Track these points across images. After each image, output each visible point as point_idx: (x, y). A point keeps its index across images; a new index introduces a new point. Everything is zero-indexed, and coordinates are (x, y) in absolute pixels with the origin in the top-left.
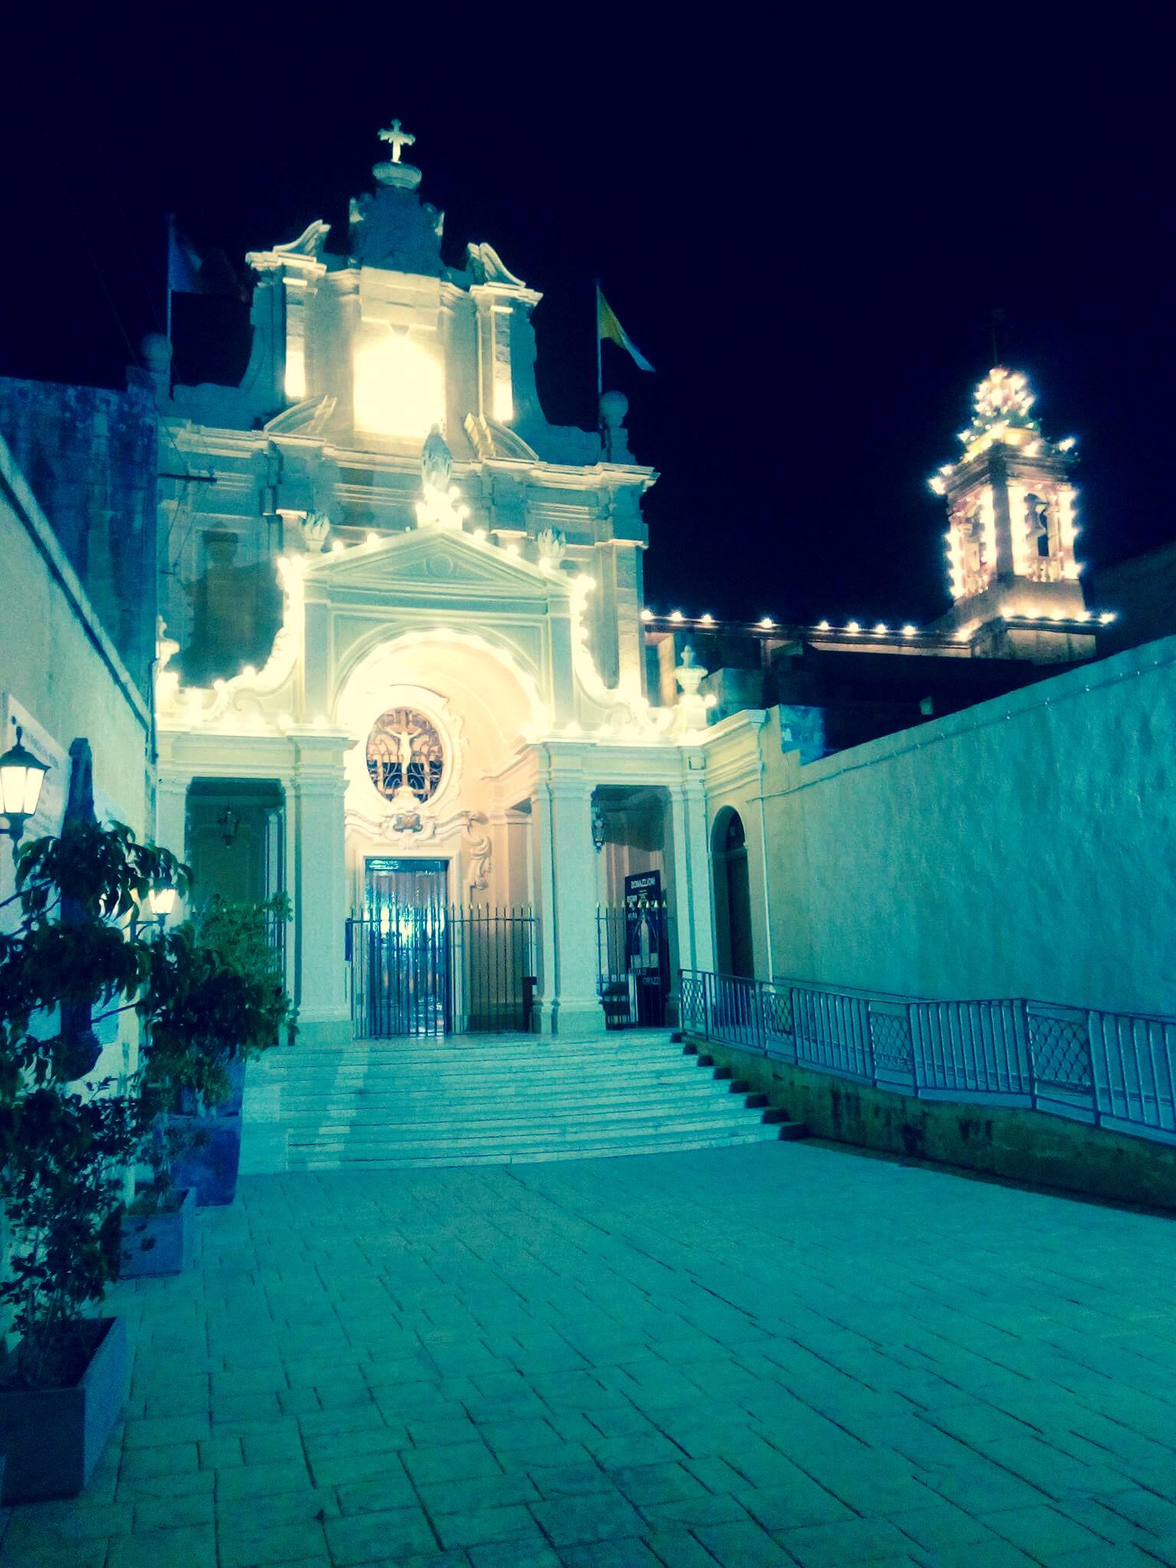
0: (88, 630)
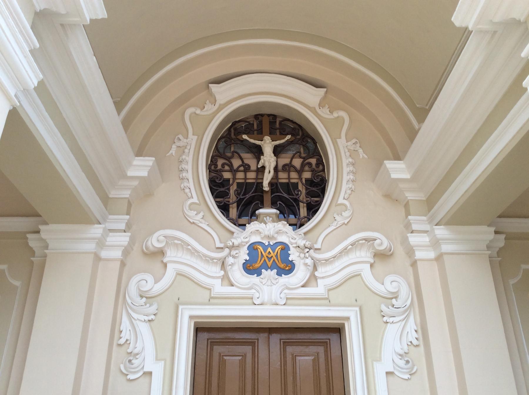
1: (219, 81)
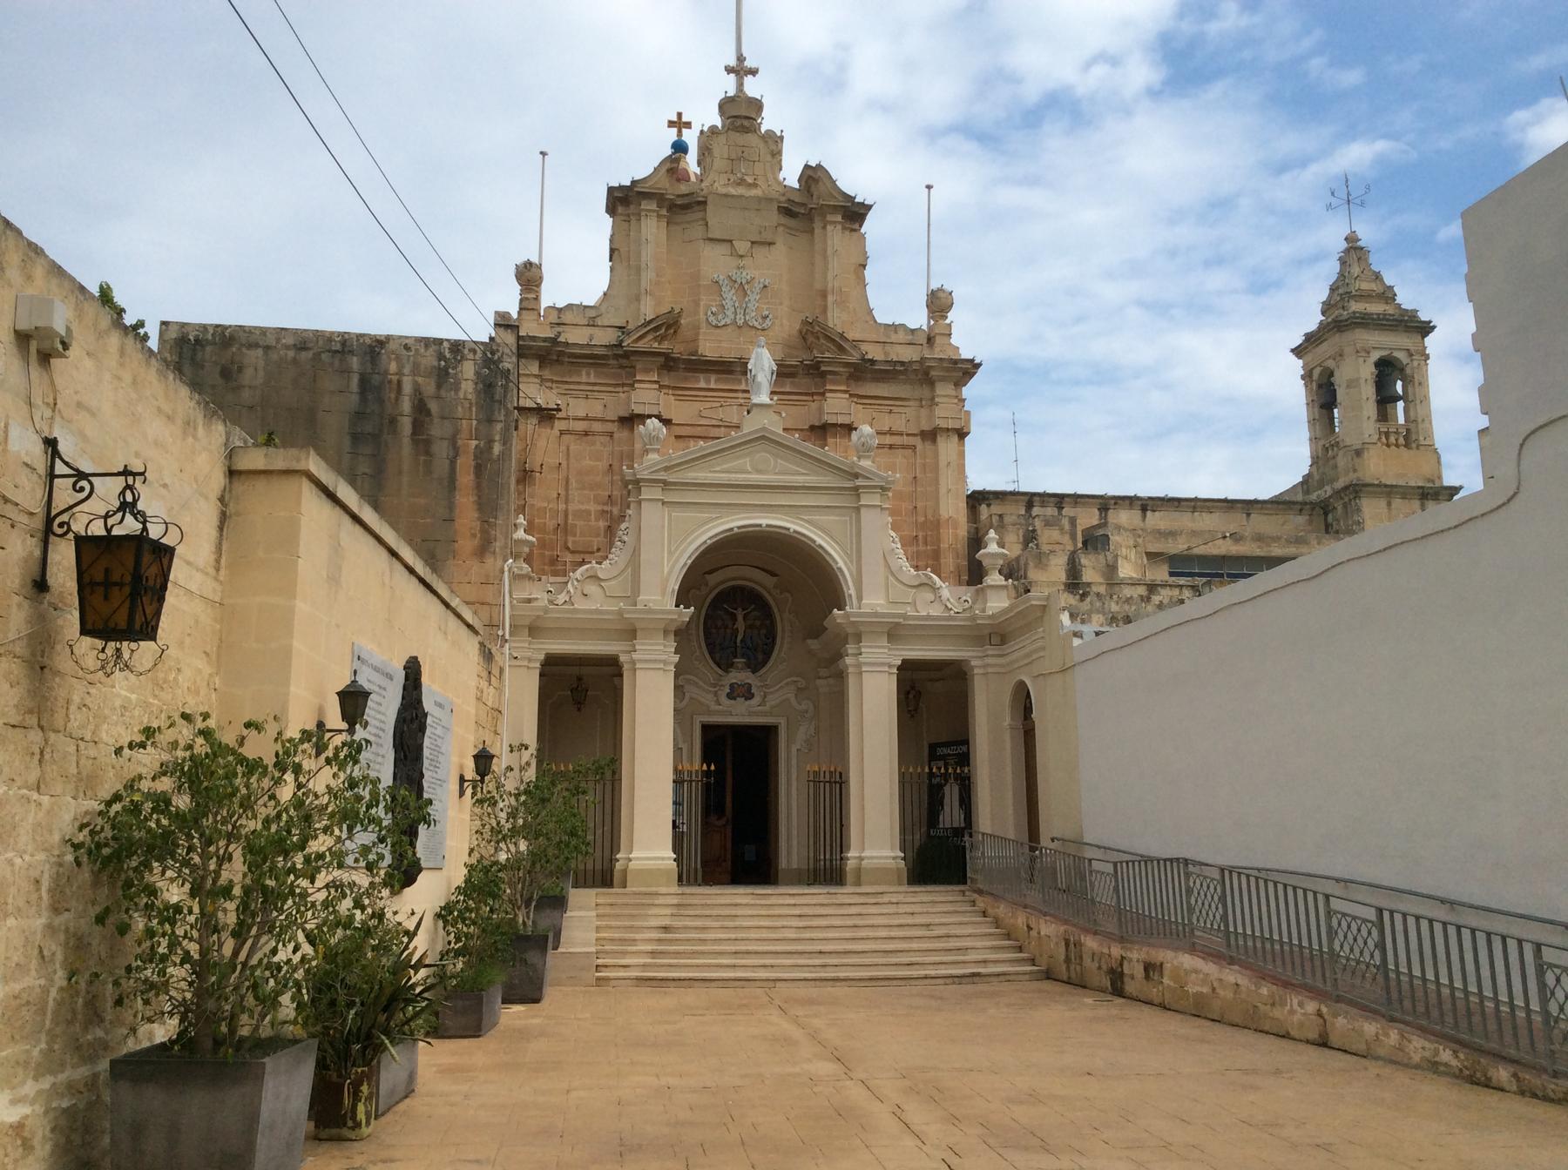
0: (422, 581)
1: (710, 572)
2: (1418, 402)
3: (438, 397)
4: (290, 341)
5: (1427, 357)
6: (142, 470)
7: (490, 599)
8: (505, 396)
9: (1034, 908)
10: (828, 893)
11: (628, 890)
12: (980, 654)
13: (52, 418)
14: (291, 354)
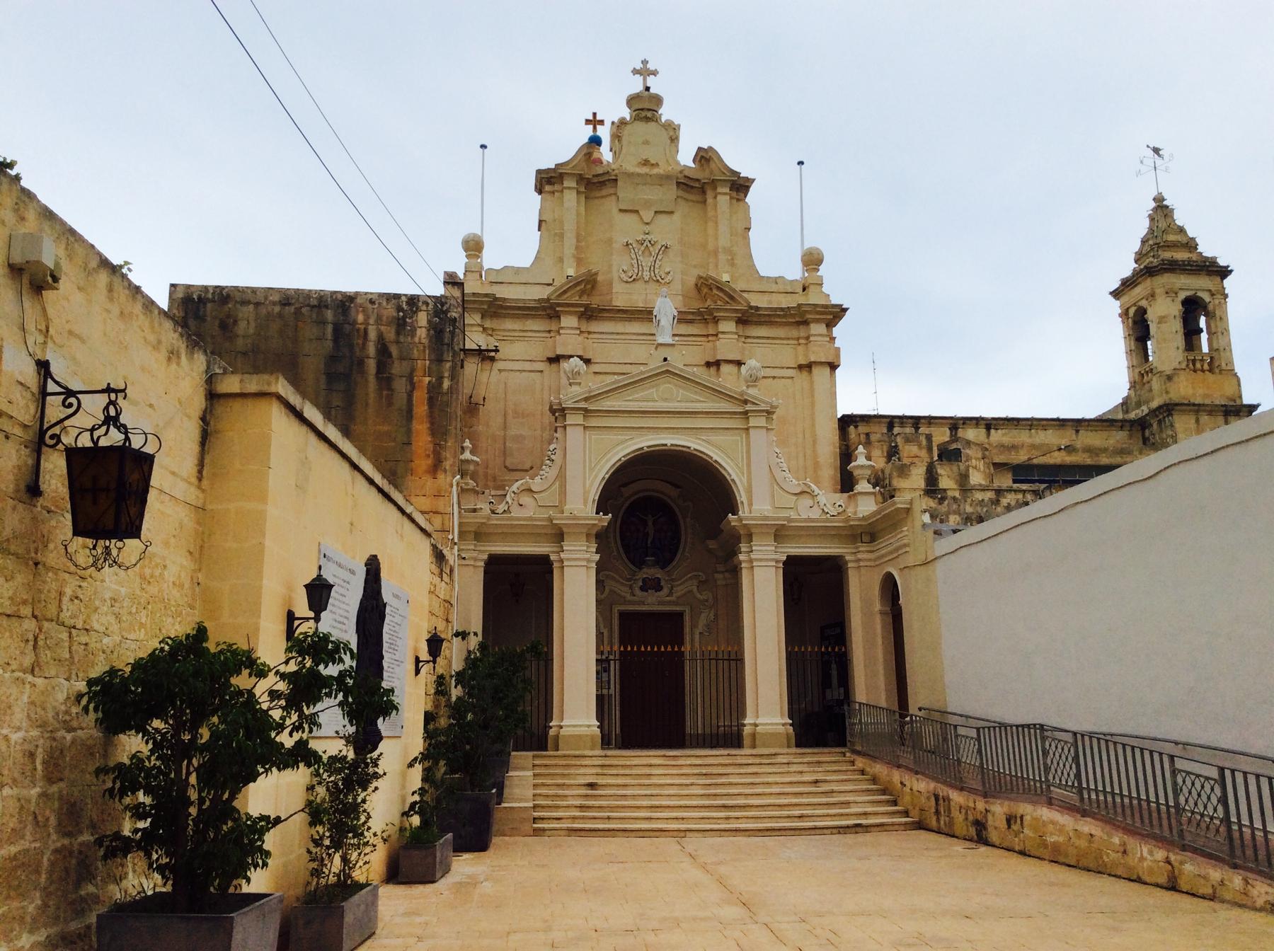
0: (380, 490)
1: (625, 485)
2: (1219, 334)
3: (398, 342)
4: (276, 298)
5: (1226, 296)
6: (123, 388)
7: (441, 509)
8: (453, 340)
9: (907, 768)
10: (728, 755)
11: (559, 753)
12: (854, 551)
13: (45, 343)
14: (277, 309)
